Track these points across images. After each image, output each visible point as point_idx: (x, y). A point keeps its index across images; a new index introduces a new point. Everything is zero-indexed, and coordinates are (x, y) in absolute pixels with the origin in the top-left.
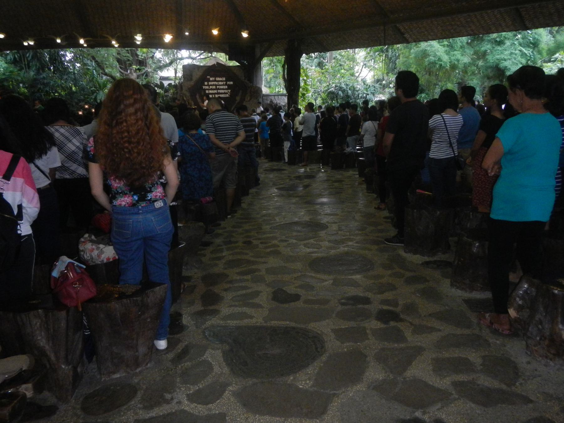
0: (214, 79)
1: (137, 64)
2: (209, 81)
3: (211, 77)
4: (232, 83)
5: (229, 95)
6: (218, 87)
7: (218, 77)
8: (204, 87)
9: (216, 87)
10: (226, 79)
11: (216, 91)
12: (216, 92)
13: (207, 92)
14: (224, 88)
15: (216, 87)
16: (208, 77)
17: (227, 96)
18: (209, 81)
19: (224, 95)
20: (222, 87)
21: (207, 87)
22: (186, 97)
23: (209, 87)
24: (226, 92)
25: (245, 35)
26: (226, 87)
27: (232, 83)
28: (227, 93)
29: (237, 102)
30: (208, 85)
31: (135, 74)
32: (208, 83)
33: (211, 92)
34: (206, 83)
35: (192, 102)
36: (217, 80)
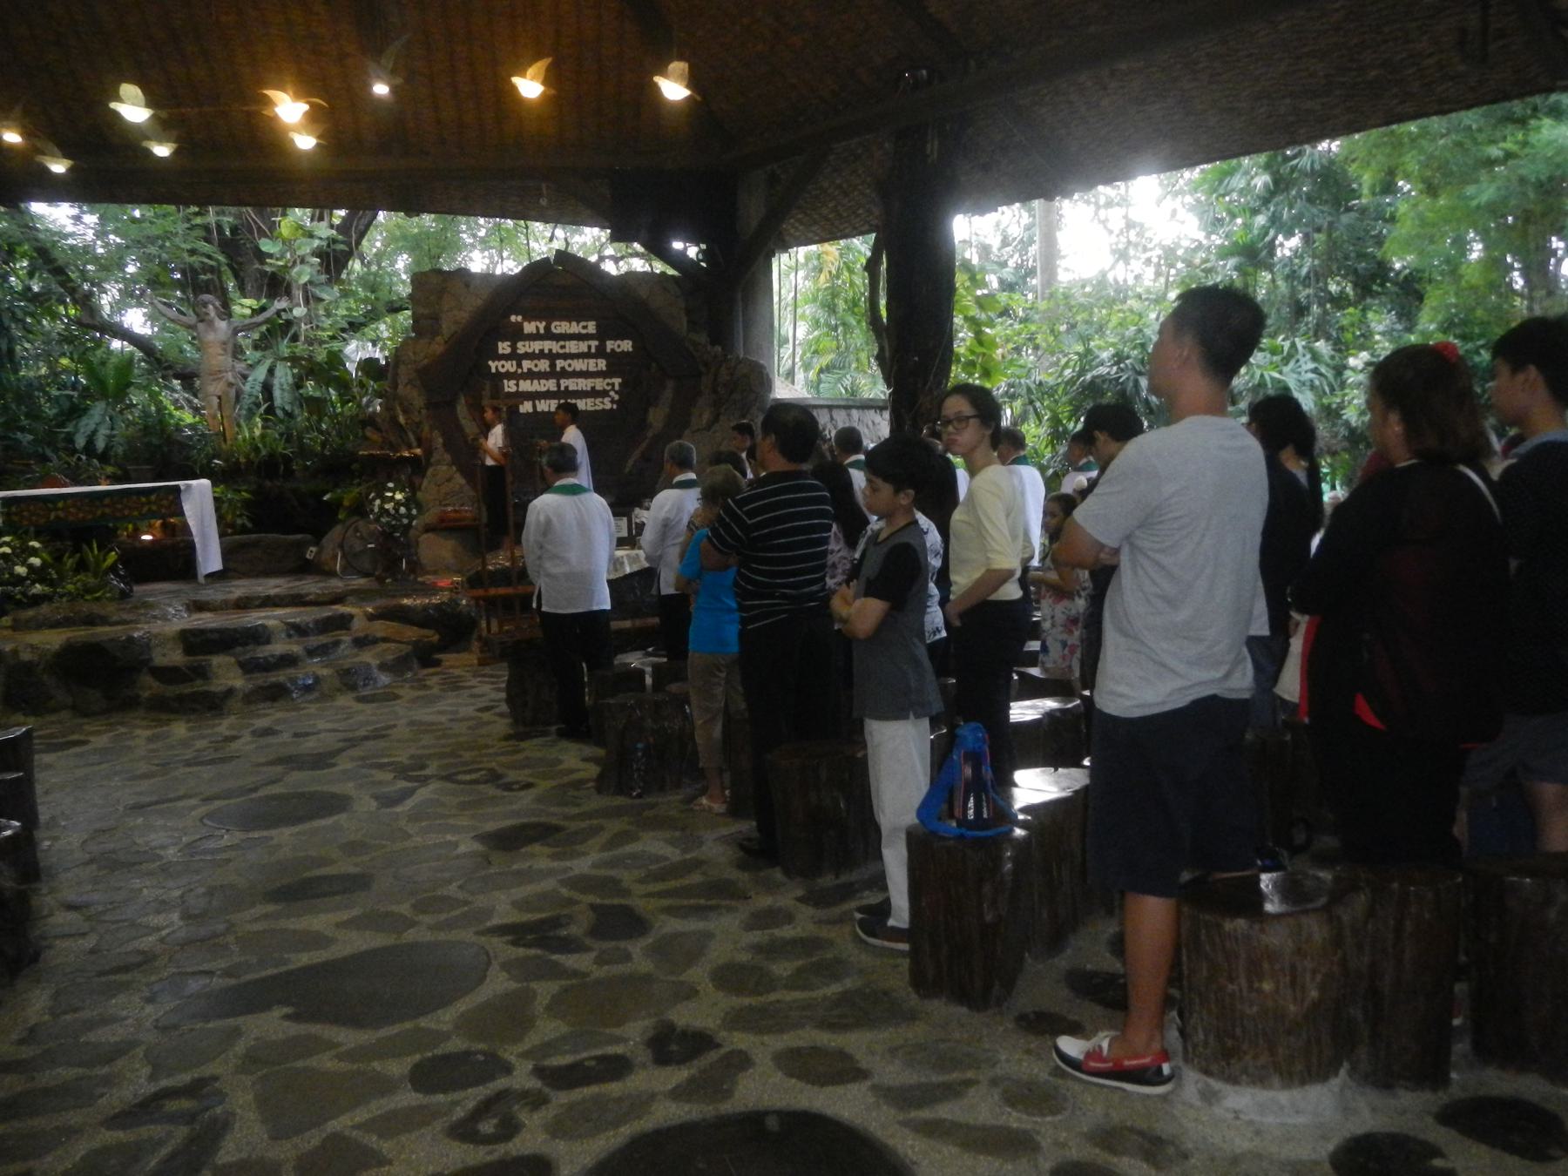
0: (542, 326)
1: (260, 289)
2: (517, 335)
3: (529, 317)
4: (626, 345)
5: (613, 401)
6: (560, 364)
7: (561, 319)
8: (493, 365)
9: (553, 365)
10: (598, 327)
11: (550, 385)
12: (553, 388)
13: (510, 386)
14: (592, 369)
15: (553, 365)
16: (513, 318)
17: (607, 404)
18: (517, 335)
19: (589, 401)
20: (579, 365)
21: (510, 366)
22: (405, 411)
23: (519, 365)
24: (598, 388)
25: (673, 90)
26: (602, 364)
27: (626, 345)
28: (604, 394)
29: (650, 434)
30: (514, 356)
32: (514, 348)
33: (526, 386)
34: (504, 347)
35: (436, 433)
36: (554, 331)
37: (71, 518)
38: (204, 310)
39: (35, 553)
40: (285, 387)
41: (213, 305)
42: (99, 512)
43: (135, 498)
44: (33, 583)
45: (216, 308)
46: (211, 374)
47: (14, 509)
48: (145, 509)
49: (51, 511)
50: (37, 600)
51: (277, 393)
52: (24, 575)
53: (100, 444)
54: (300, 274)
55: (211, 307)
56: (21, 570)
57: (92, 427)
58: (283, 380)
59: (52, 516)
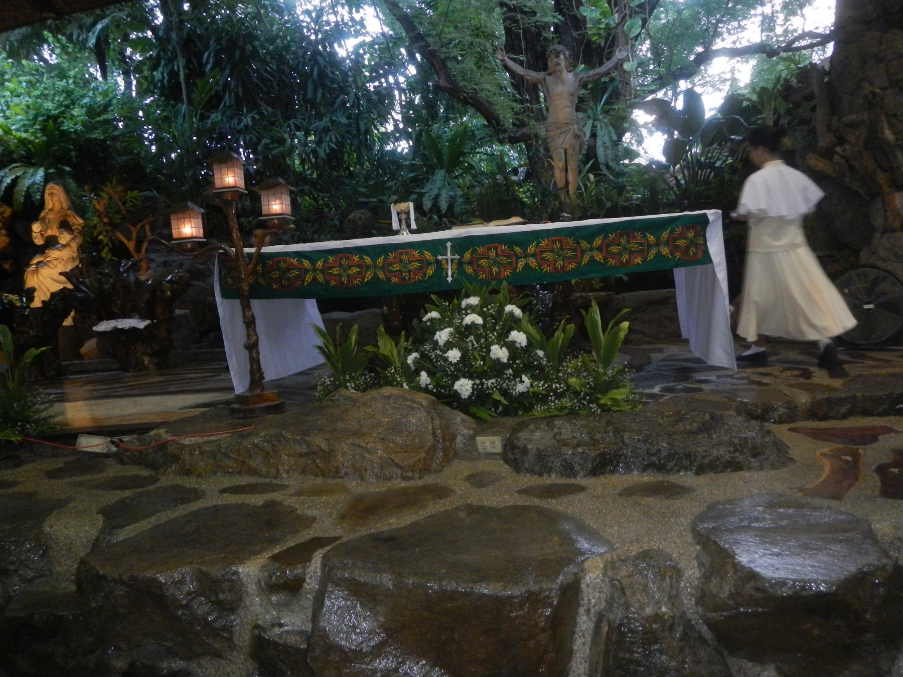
31: (569, 77)
37: (547, 269)
38: (556, 60)
39: (514, 323)
40: (608, 144)
41: (564, 54)
42: (586, 258)
43: (638, 235)
44: (517, 375)
45: (566, 58)
46: (559, 128)
47: (467, 256)
48: (654, 251)
49: (518, 258)
50: (525, 402)
51: (600, 151)
52: (505, 360)
53: (444, 205)
54: (630, 28)
55: (562, 56)
56: (499, 353)
57: (436, 191)
58: (606, 139)
59: (521, 263)
